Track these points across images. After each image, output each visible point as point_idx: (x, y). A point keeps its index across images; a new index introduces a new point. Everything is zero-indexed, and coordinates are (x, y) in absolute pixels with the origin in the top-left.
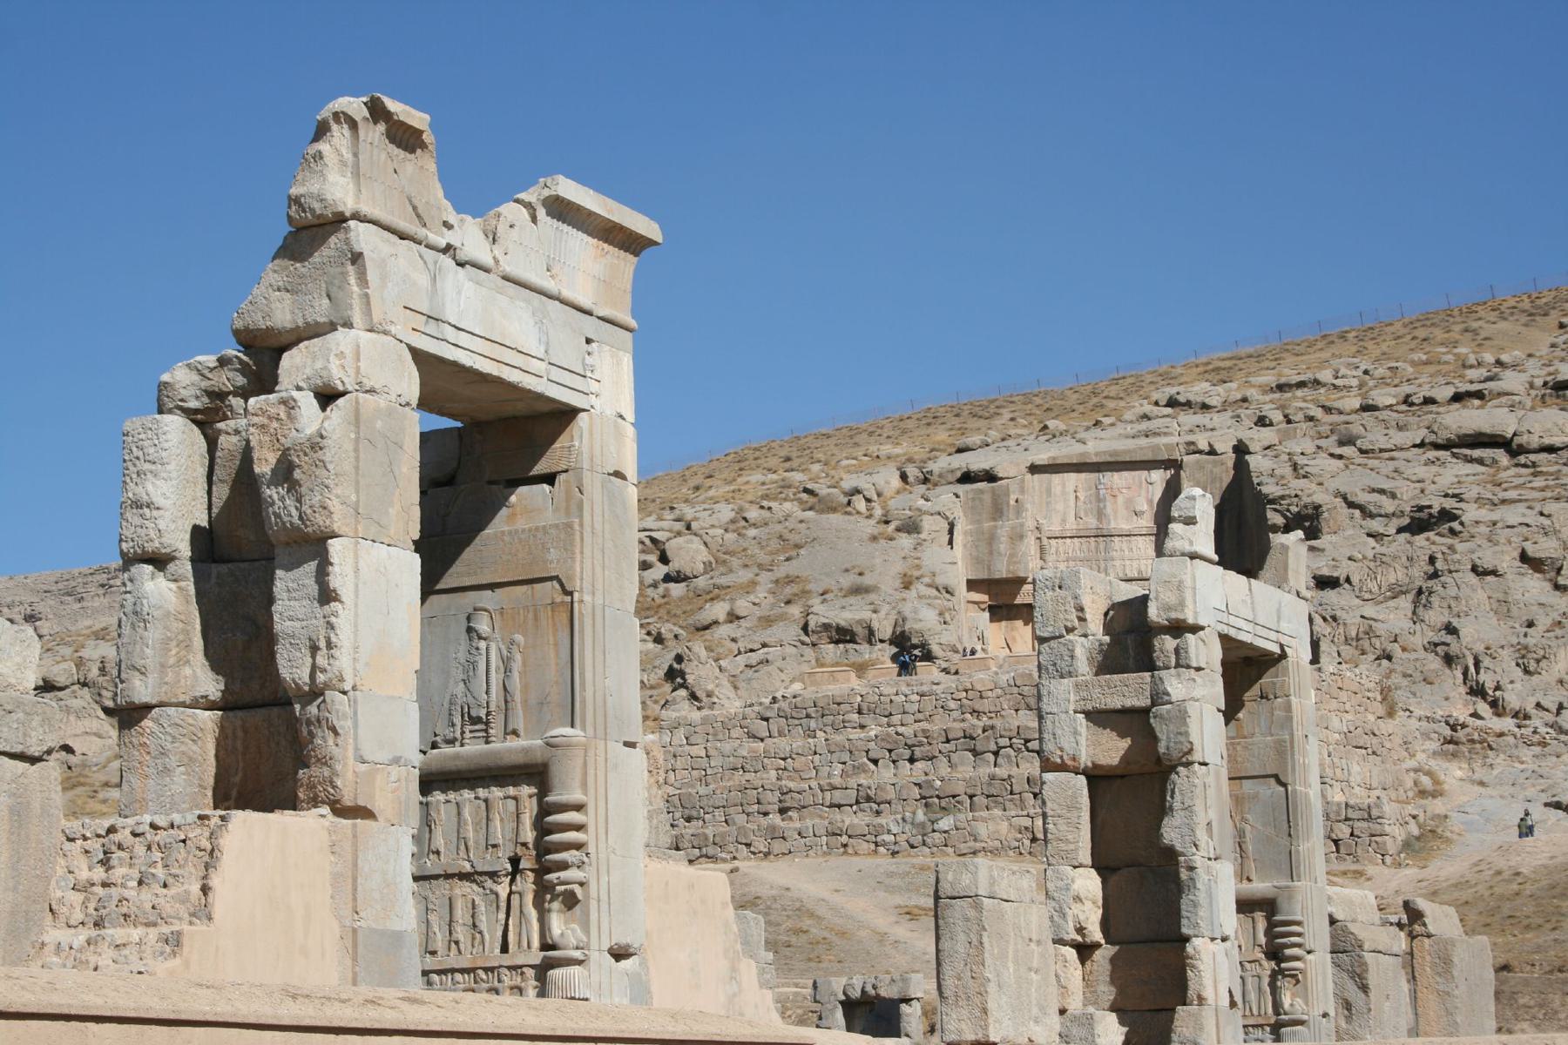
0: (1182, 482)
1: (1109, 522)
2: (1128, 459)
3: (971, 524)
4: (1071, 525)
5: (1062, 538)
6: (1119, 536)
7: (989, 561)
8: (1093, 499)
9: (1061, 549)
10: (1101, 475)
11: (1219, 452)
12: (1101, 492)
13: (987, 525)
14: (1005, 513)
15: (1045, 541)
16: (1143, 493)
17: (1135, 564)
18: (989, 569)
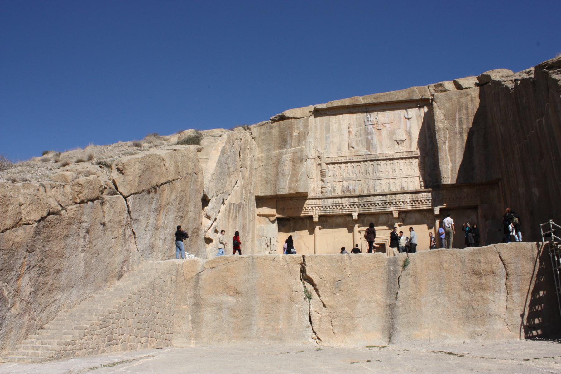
0: (434, 110)
1: (376, 148)
2: (389, 100)
3: (262, 152)
4: (346, 152)
5: (338, 163)
6: (384, 160)
7: (276, 181)
8: (362, 132)
9: (337, 173)
10: (368, 114)
11: (464, 87)
12: (369, 127)
13: (275, 152)
14: (289, 141)
15: (324, 166)
16: (402, 126)
17: (398, 181)
18: (275, 187)
